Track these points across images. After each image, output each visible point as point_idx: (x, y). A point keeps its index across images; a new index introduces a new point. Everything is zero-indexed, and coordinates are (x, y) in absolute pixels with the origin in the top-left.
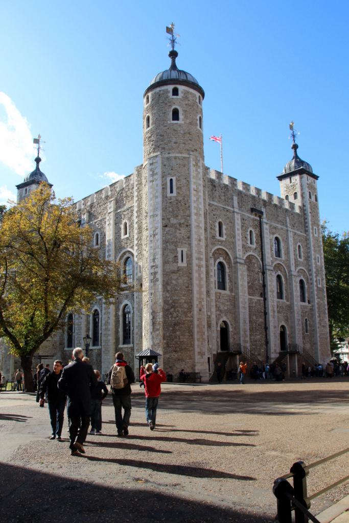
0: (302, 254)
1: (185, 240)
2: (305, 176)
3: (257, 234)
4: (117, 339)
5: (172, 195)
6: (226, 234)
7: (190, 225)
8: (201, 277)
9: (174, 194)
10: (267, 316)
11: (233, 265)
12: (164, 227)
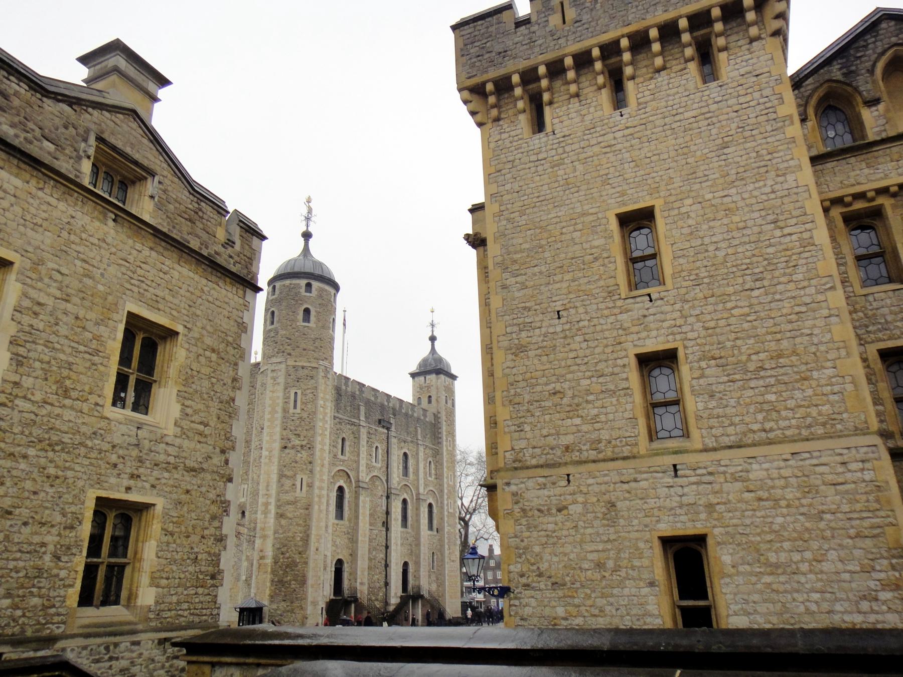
0: (433, 472)
2: (442, 377)
3: (383, 450)
5: (295, 411)
9: (298, 410)
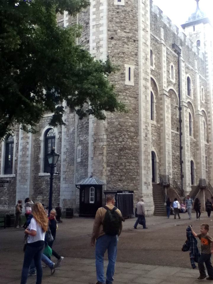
1: (132, 56)
4: (36, 168)
6: (155, 64)
7: (138, 41)
8: (147, 99)
10: (182, 150)
11: (159, 96)
12: (109, 39)
